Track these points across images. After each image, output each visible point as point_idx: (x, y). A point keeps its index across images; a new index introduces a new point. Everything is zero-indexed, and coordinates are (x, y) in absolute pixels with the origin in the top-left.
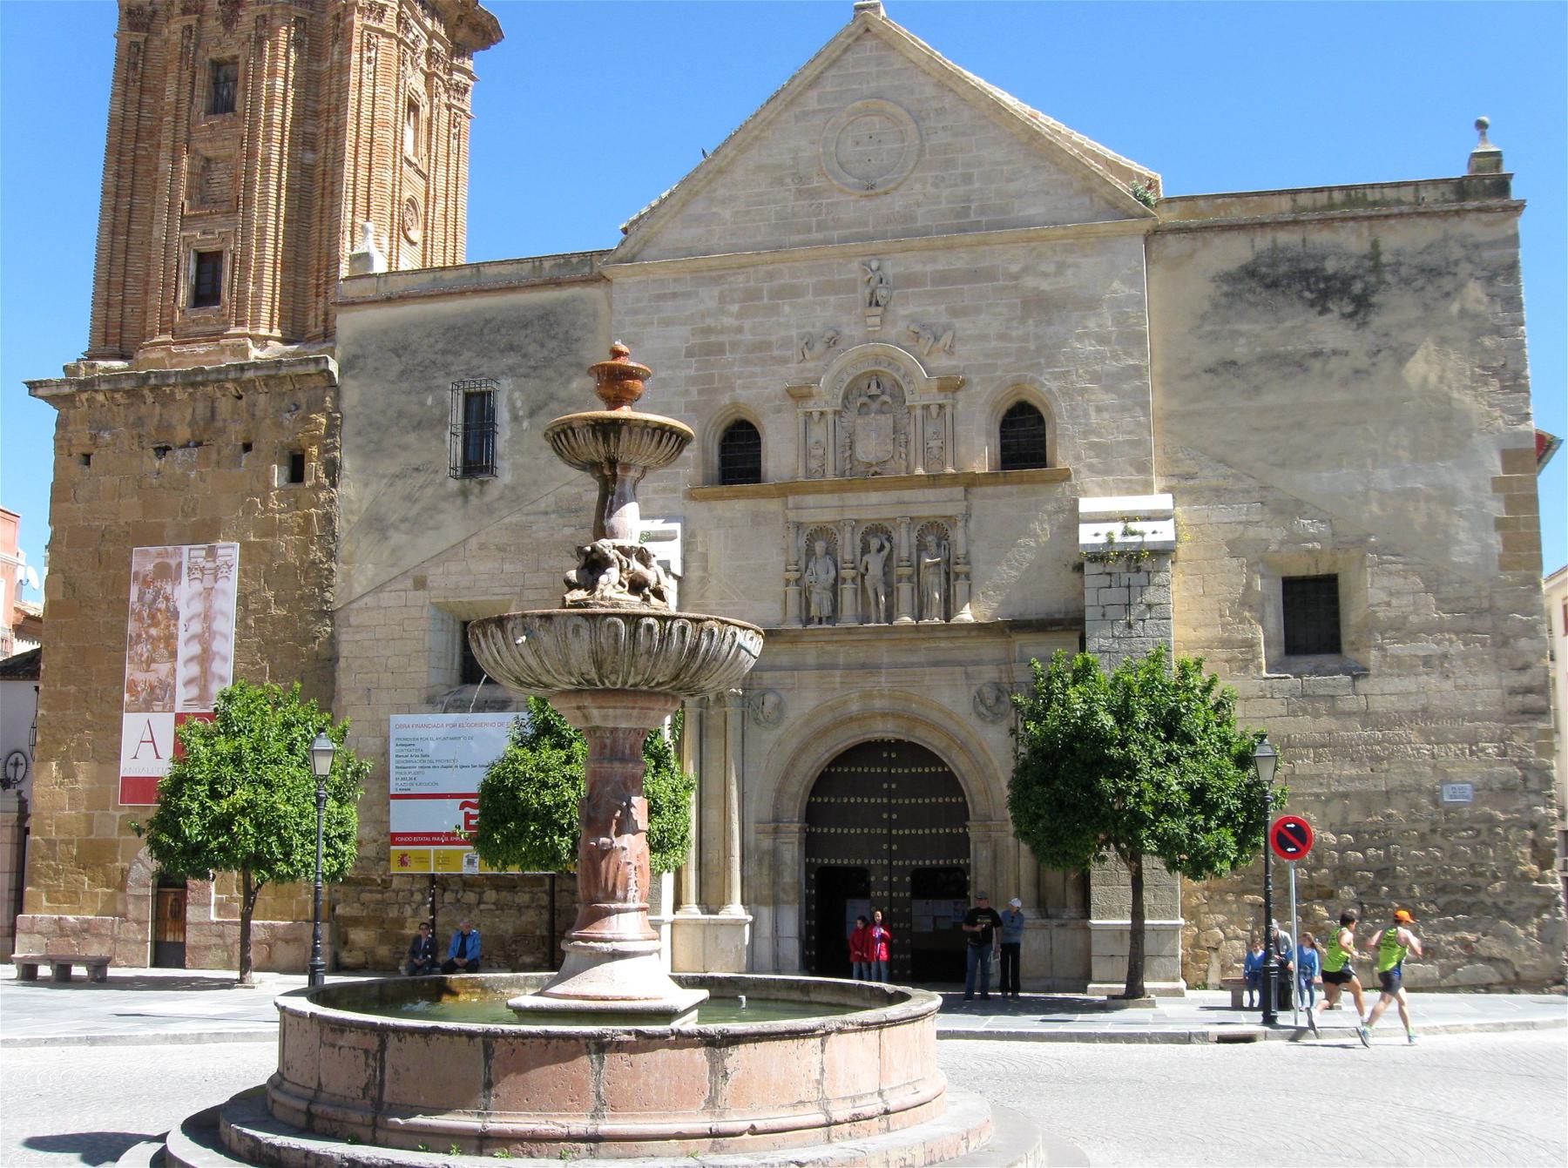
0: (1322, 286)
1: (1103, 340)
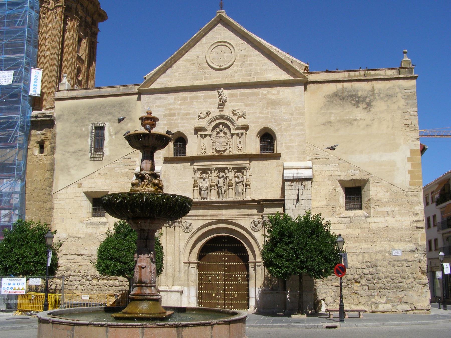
0: (357, 99)
1: (292, 114)
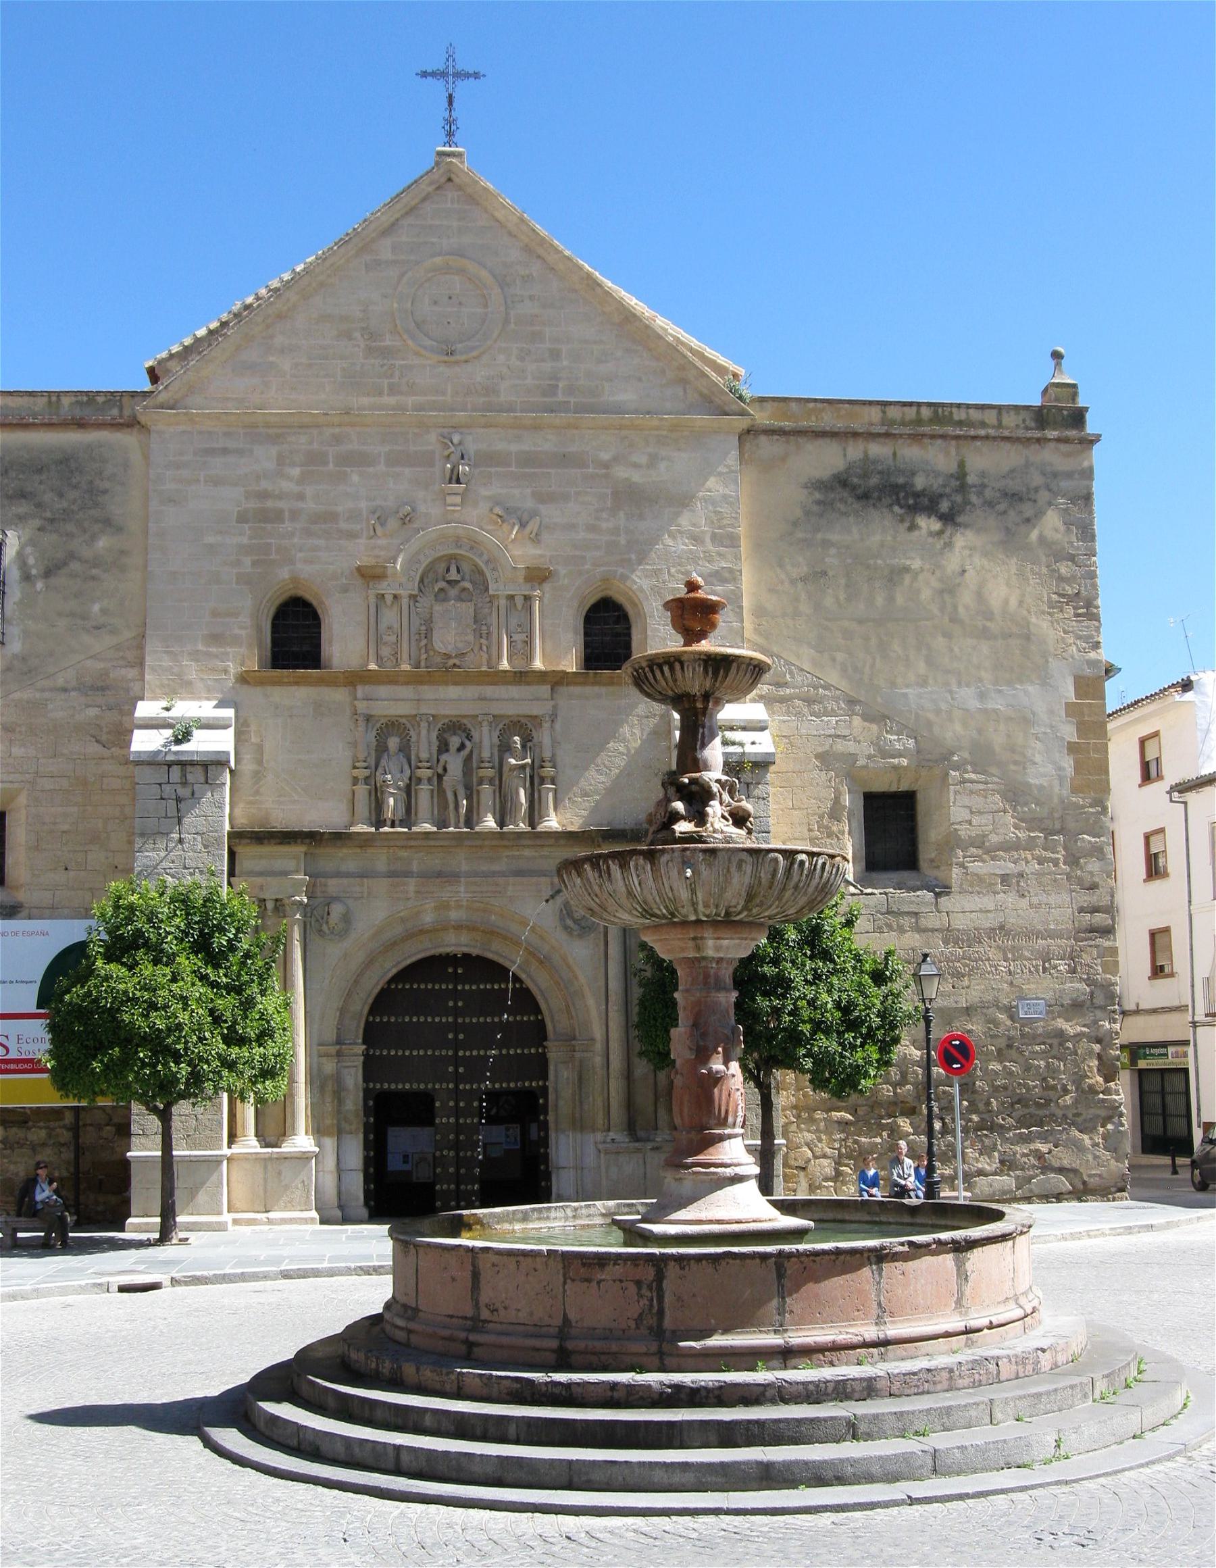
0: (911, 502)
1: (696, 539)
